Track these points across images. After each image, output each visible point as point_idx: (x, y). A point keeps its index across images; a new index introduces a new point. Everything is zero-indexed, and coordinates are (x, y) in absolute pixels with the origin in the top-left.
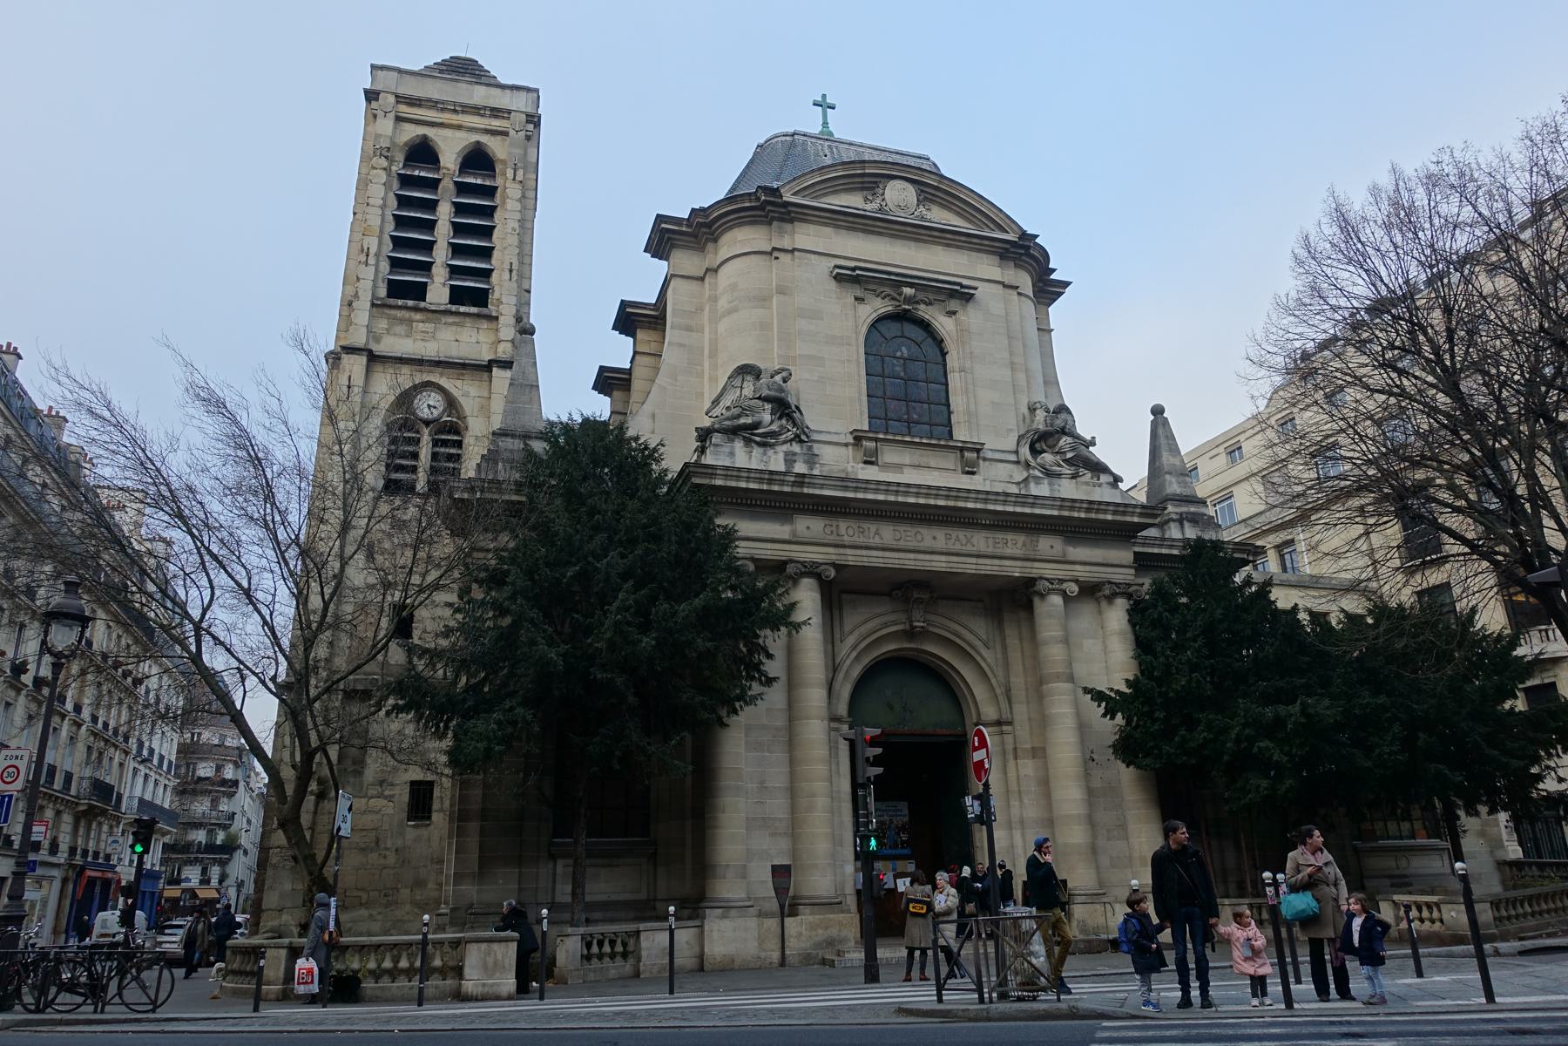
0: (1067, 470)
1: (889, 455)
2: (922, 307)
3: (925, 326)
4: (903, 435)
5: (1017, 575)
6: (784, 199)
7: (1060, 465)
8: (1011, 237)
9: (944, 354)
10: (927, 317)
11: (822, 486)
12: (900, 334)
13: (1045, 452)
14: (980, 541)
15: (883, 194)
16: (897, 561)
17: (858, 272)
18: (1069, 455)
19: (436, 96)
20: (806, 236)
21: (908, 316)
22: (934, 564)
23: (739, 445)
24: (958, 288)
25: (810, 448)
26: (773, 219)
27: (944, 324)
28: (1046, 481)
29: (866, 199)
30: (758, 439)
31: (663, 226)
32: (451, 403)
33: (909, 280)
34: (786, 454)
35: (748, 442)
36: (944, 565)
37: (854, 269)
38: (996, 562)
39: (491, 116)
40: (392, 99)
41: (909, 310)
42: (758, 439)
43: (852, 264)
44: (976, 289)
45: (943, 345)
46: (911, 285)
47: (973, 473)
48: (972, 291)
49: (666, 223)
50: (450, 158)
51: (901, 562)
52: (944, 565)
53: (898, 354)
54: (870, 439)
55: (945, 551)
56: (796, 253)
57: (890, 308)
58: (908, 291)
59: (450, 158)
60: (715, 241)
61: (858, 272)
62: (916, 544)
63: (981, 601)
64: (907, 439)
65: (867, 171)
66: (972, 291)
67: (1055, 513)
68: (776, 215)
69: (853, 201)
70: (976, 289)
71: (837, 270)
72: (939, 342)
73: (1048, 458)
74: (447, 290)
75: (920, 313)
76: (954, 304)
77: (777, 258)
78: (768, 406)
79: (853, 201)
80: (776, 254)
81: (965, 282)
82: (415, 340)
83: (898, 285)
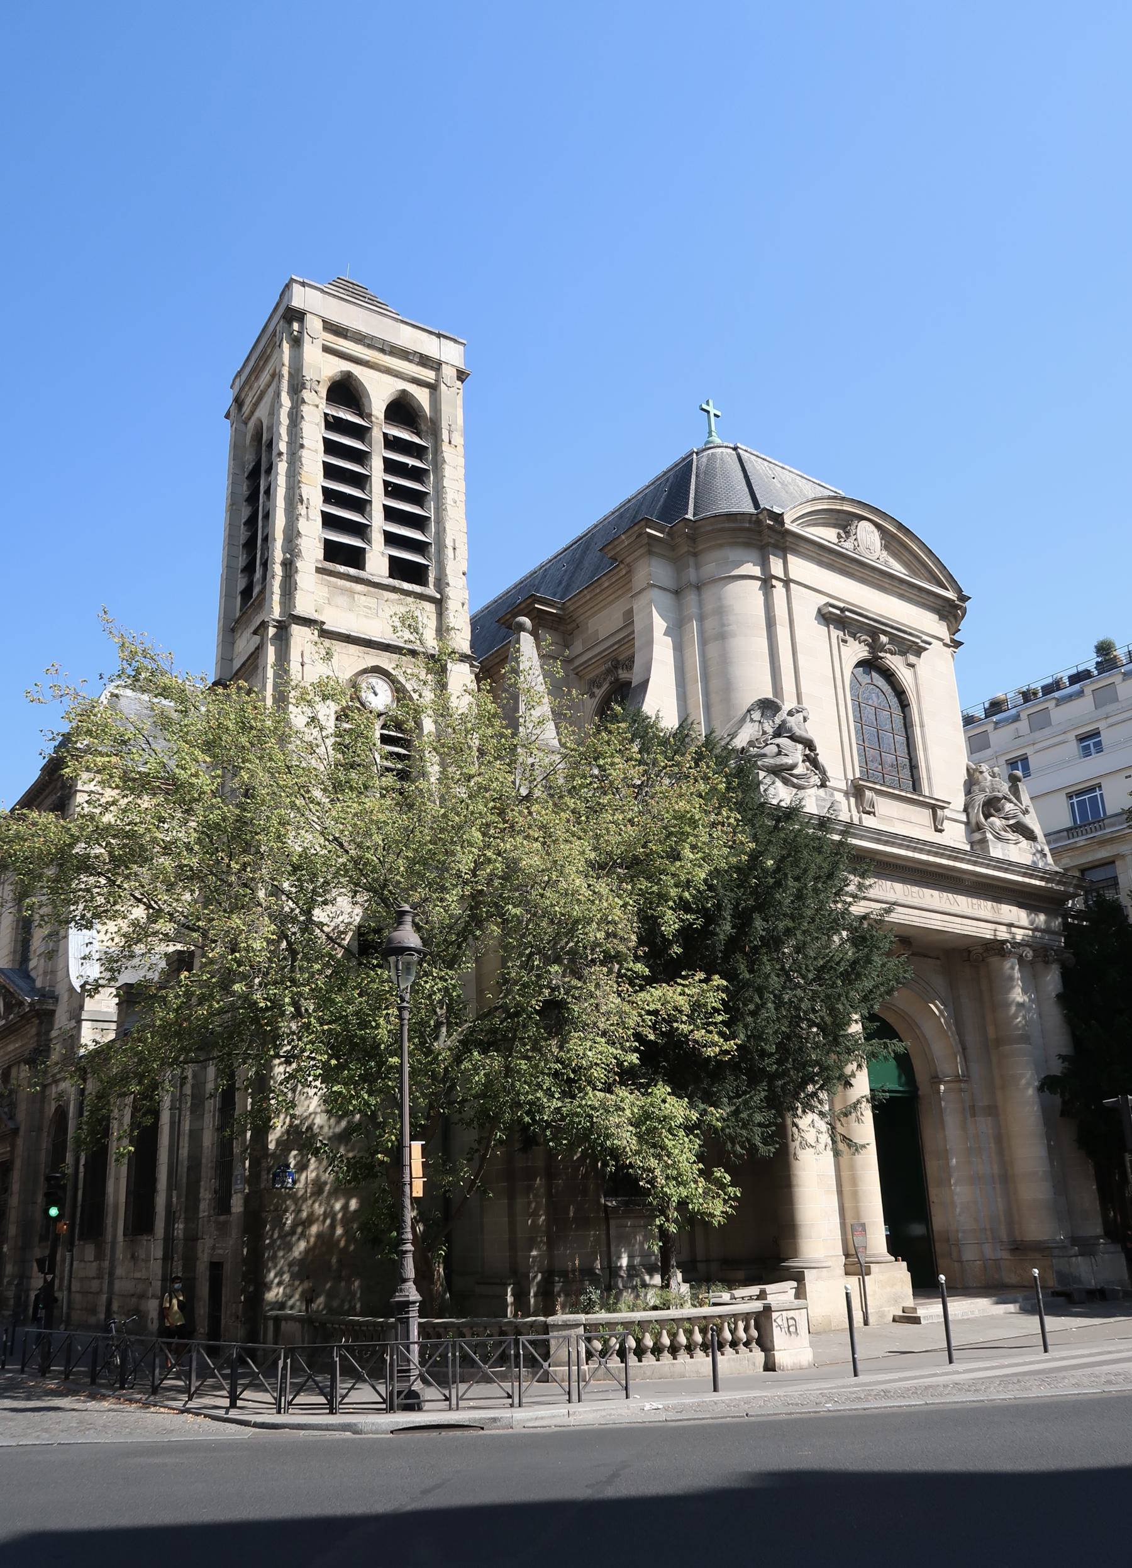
0: (1011, 836)
1: (884, 806)
2: (888, 655)
3: (889, 675)
4: (894, 788)
5: (988, 937)
6: (786, 526)
7: (1006, 831)
8: (951, 595)
9: (904, 705)
10: (893, 667)
11: (862, 838)
12: (870, 681)
13: (993, 816)
14: (963, 903)
15: (855, 534)
16: (907, 917)
17: (847, 613)
18: (1012, 822)
19: (364, 329)
20: (800, 568)
21: (876, 663)
22: (932, 922)
23: (779, 783)
24: (918, 641)
25: (832, 795)
26: (768, 544)
27: (905, 675)
28: (1000, 844)
29: (839, 536)
30: (795, 781)
31: (648, 530)
32: (400, 692)
33: (884, 628)
34: (818, 798)
35: (786, 782)
36: (939, 923)
37: (842, 610)
38: (975, 923)
39: (418, 364)
40: (319, 324)
41: (881, 658)
42: (795, 781)
43: (842, 605)
44: (930, 644)
45: (903, 697)
46: (885, 633)
47: (941, 831)
48: (927, 646)
49: (650, 528)
50: (378, 406)
51: (910, 918)
52: (939, 923)
53: (870, 702)
54: (871, 789)
55: (941, 909)
56: (792, 584)
57: (866, 654)
58: (884, 639)
59: (378, 406)
60: (695, 555)
61: (847, 613)
62: (920, 901)
63: (938, 958)
64: (897, 792)
65: (845, 508)
66: (927, 646)
67: (1020, 879)
68: (772, 541)
69: (827, 535)
70: (930, 644)
71: (831, 609)
72: (900, 694)
73: (997, 822)
74: (386, 561)
75: (887, 662)
76: (912, 659)
77: (774, 587)
78: (800, 747)
79: (827, 535)
80: (774, 582)
81: (925, 638)
82: (358, 615)
83: (874, 633)
